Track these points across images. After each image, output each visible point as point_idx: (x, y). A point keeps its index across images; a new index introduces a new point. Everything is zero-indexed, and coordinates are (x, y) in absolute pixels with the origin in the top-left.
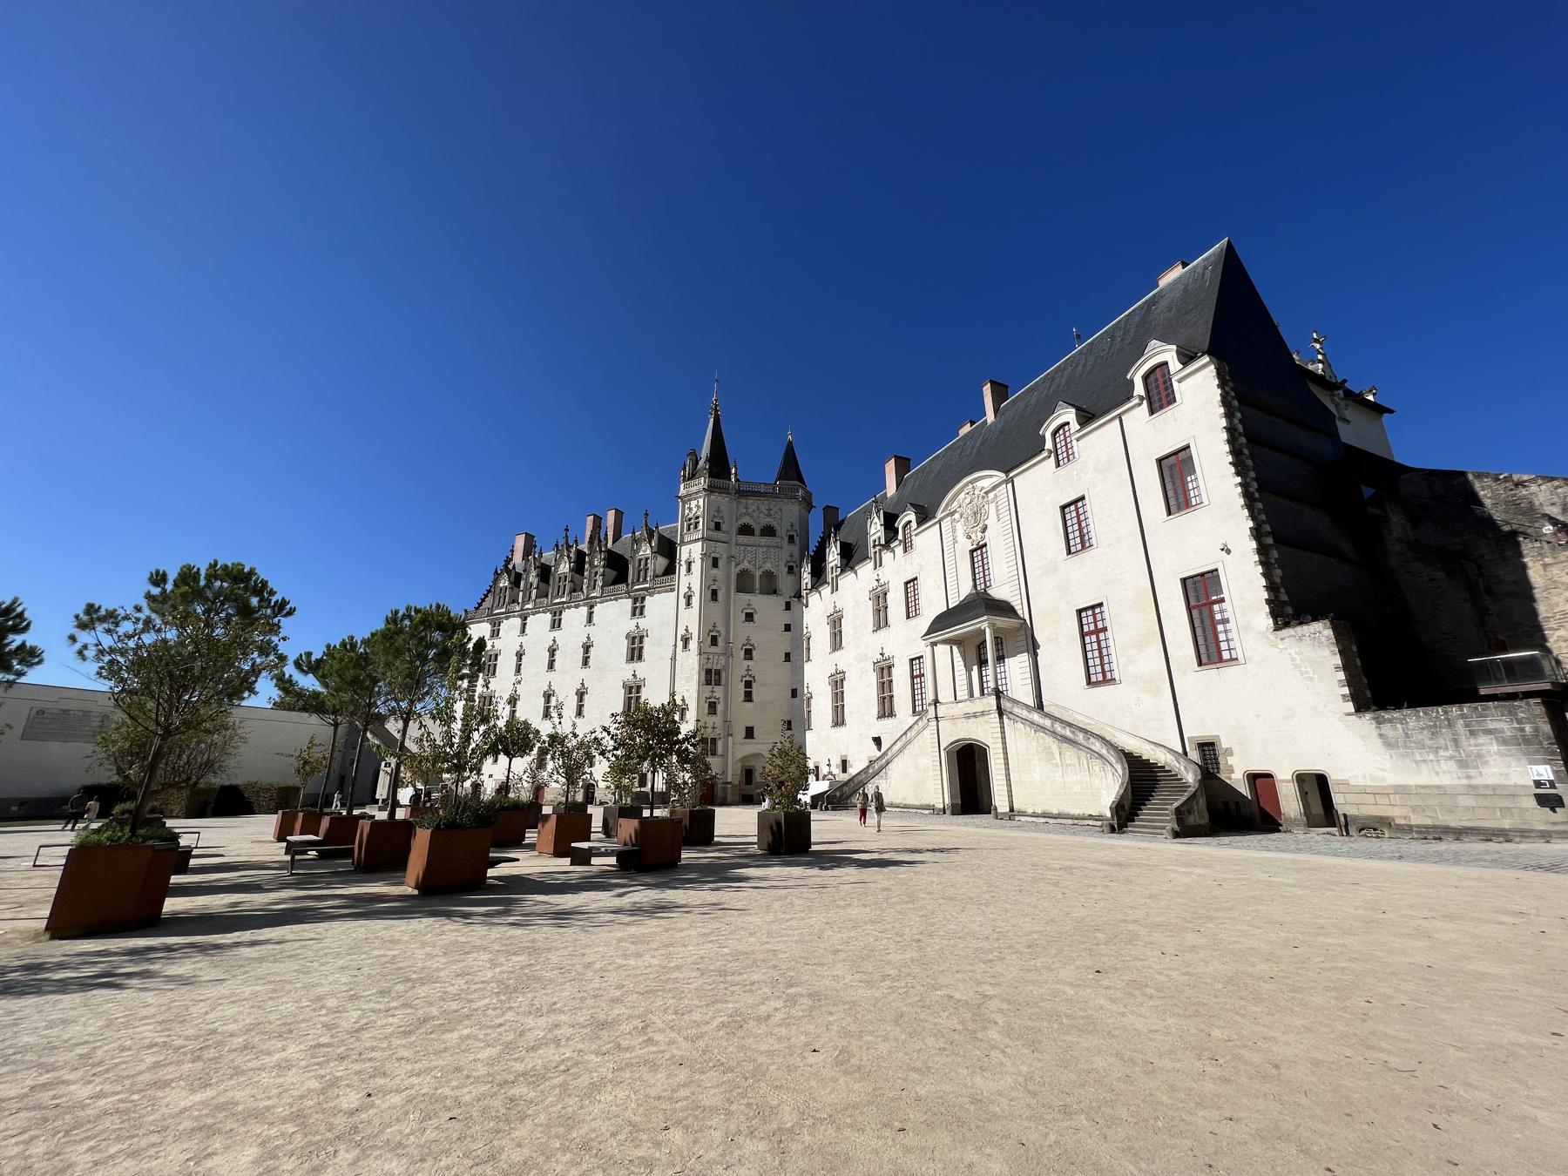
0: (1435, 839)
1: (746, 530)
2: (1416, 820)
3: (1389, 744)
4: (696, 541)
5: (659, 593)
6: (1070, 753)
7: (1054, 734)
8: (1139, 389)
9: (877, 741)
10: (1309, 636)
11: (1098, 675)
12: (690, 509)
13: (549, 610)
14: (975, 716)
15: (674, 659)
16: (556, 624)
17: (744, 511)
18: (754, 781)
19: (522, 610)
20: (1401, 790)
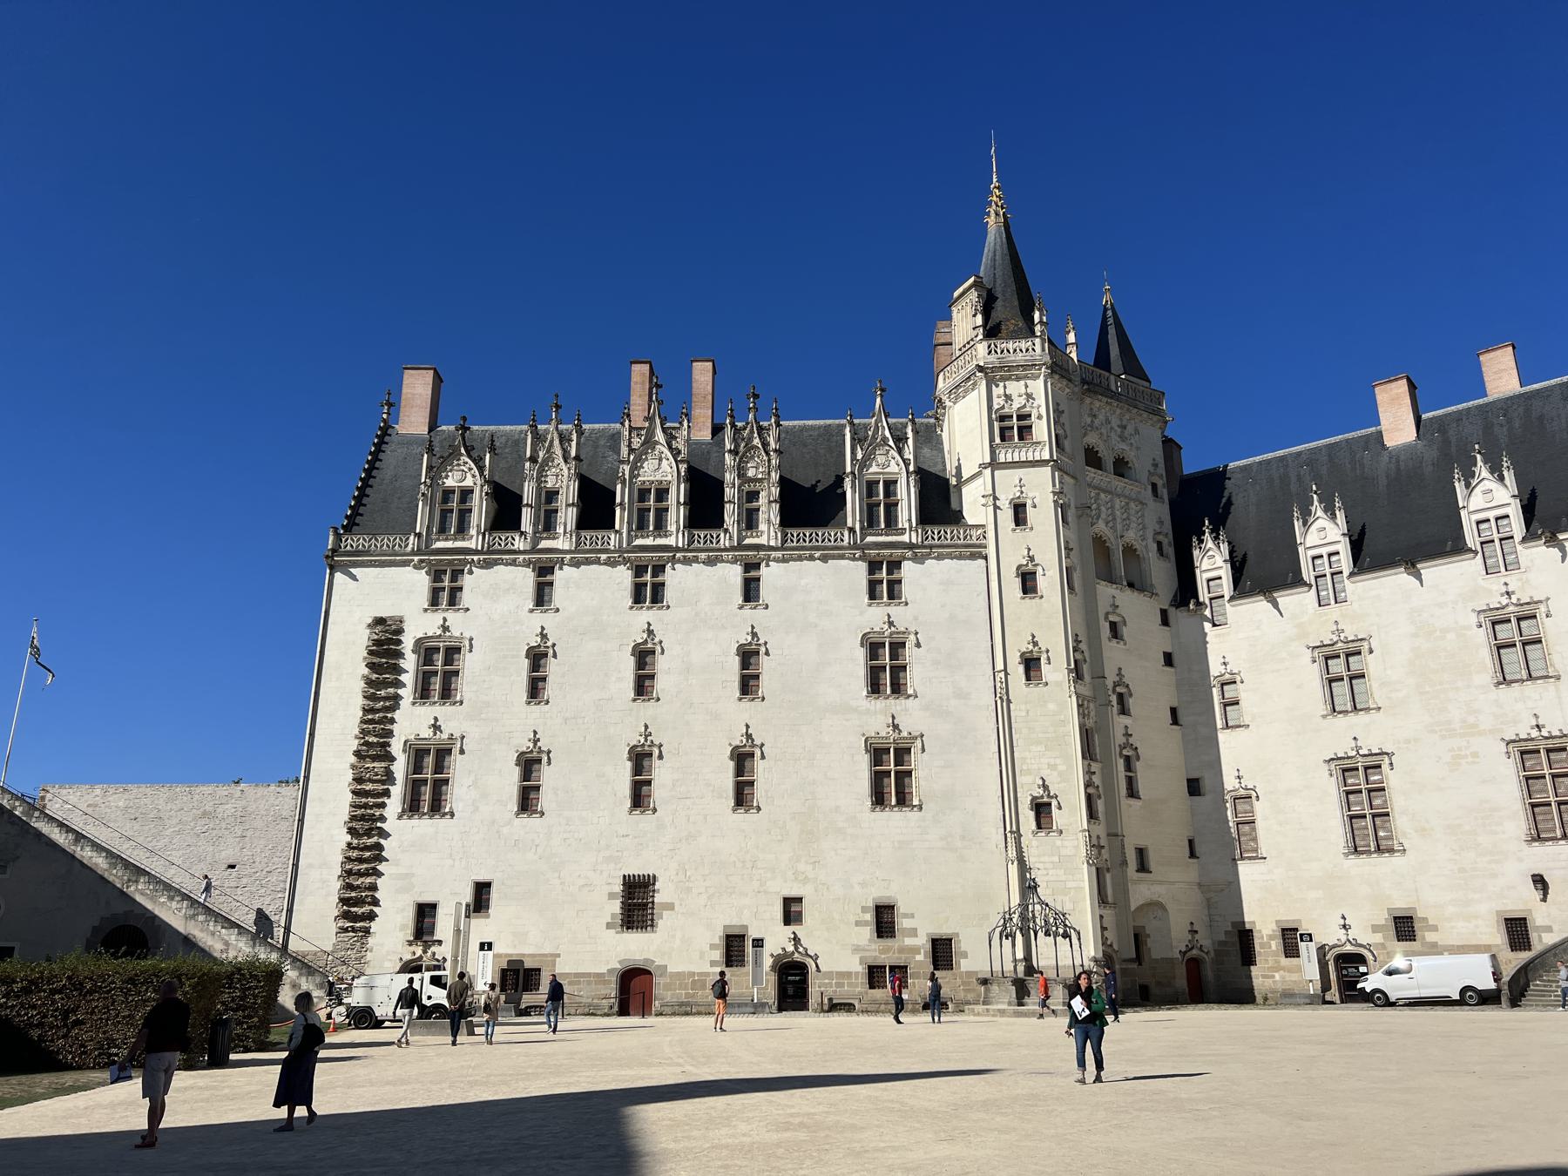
5: (940, 557)
9: (1540, 882)
12: (1008, 398)
13: (625, 561)
15: (1004, 699)
16: (648, 592)
17: (1089, 420)
18: (1146, 958)
19: (534, 550)
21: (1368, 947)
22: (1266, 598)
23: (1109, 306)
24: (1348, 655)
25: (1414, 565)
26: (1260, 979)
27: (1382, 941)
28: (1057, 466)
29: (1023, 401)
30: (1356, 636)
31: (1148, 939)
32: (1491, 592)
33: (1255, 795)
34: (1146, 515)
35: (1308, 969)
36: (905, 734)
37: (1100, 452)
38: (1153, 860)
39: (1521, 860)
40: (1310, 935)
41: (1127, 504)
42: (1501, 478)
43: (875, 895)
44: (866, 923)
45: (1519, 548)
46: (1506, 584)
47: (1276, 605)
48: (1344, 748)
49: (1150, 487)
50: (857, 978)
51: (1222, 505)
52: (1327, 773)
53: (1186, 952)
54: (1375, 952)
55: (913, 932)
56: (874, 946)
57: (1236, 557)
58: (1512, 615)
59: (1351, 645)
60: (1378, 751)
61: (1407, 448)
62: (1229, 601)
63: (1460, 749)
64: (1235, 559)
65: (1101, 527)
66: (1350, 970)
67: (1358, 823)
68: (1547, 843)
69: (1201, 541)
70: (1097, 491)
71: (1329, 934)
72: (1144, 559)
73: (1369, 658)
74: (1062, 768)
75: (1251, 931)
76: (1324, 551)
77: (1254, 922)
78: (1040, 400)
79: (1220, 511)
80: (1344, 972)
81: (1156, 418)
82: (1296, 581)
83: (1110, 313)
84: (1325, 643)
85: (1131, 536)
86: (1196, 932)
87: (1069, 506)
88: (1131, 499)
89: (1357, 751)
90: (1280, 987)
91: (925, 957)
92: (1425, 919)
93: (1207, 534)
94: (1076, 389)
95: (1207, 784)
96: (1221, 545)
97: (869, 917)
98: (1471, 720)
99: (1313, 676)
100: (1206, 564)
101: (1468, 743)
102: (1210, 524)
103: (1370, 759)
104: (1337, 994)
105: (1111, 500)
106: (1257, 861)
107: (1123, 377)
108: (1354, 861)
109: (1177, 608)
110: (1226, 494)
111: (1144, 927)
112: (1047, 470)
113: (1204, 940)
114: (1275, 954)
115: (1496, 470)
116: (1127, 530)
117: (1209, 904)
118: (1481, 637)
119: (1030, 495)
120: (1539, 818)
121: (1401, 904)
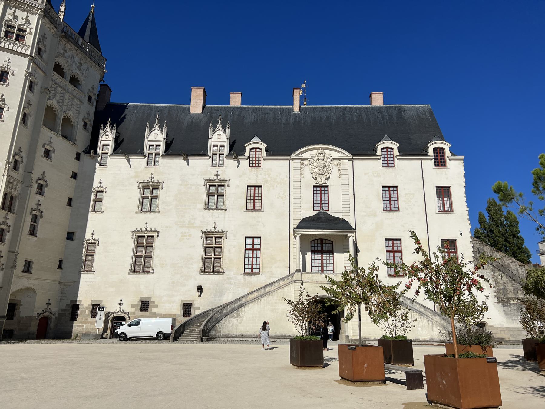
0: (516, 344)
1: (58, 69)
2: (511, 339)
3: (506, 314)
4: (25, 55)
8: (431, 152)
9: (200, 289)
10: (486, 273)
17: (62, 52)
18: (17, 316)
20: (508, 329)
21: (128, 314)
22: (126, 158)
23: (92, 13)
24: (153, 189)
25: (187, 157)
26: (77, 327)
27: (134, 311)
28: (32, 59)
29: (23, 22)
30: (158, 181)
31: (21, 307)
33: (98, 243)
34: (81, 107)
35: (99, 322)
37: (65, 69)
38: (34, 268)
39: (195, 279)
40: (104, 307)
41: (73, 98)
42: (225, 131)
45: (225, 159)
46: (217, 171)
47: (129, 162)
48: (141, 227)
49: (87, 97)
51: (121, 118)
52: (131, 236)
53: (41, 314)
54: (130, 316)
57: (119, 139)
58: (216, 183)
59: (155, 184)
60: (154, 230)
61: (197, 115)
62: (110, 156)
63: (185, 233)
64: (119, 140)
65: (54, 103)
66: (118, 324)
67: (138, 260)
68: (206, 274)
69: (105, 127)
70: (57, 85)
71: (112, 307)
72: (75, 127)
75: (79, 304)
76: (155, 143)
77: (81, 301)
78: (33, 25)
79: (119, 120)
80: (115, 325)
81: (99, 68)
83: (91, 16)
84: (145, 182)
85: (70, 114)
86: (50, 304)
87: (37, 84)
88: (75, 97)
89: (146, 229)
90: (84, 331)
92: (154, 302)
93: (108, 125)
94: (58, 33)
95: (76, 236)
96: (113, 131)
98: (192, 222)
99: (136, 194)
100: (104, 138)
101: (189, 231)
102: (111, 120)
103: (150, 233)
104: (109, 335)
105: (64, 93)
106: (90, 273)
107: (88, 43)
108: (132, 275)
109: (85, 154)
110: (124, 114)
111: (20, 300)
112: (26, 60)
113: (54, 308)
114: (87, 316)
115: (224, 128)
116: (69, 110)
117: (62, 291)
118: (204, 189)
119: (12, 68)
120: (206, 263)
121: (145, 295)
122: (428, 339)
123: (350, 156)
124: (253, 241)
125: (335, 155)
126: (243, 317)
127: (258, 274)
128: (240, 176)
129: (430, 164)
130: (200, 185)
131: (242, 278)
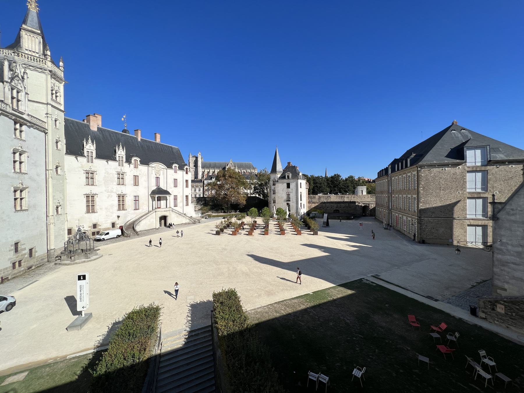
6: (180, 216)
7: (178, 214)
9: (118, 217)
11: (176, 206)
14: (167, 211)
32: (119, 169)
36: (24, 186)
43: (15, 240)
44: (12, 250)
47: (77, 159)
48: (88, 192)
50: (9, 269)
55: (25, 249)
56: (15, 256)
63: (110, 195)
73: (96, 175)
74: (63, 198)
82: (82, 155)
91: (28, 255)
92: (99, 224)
97: (13, 248)
98: (112, 190)
99: (84, 176)
118: (116, 176)
121: (95, 222)
122: (185, 223)
123: (167, 168)
124: (136, 197)
125: (162, 167)
126: (141, 225)
127: (138, 209)
128: (131, 171)
129: (185, 173)
130: (114, 174)
131: (133, 211)
